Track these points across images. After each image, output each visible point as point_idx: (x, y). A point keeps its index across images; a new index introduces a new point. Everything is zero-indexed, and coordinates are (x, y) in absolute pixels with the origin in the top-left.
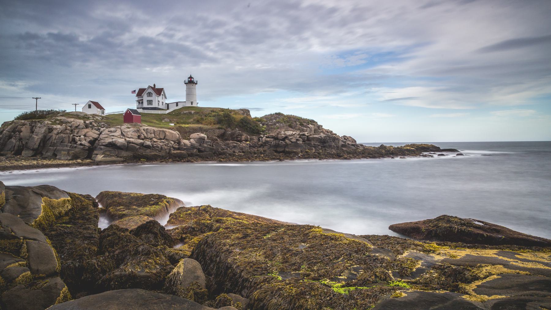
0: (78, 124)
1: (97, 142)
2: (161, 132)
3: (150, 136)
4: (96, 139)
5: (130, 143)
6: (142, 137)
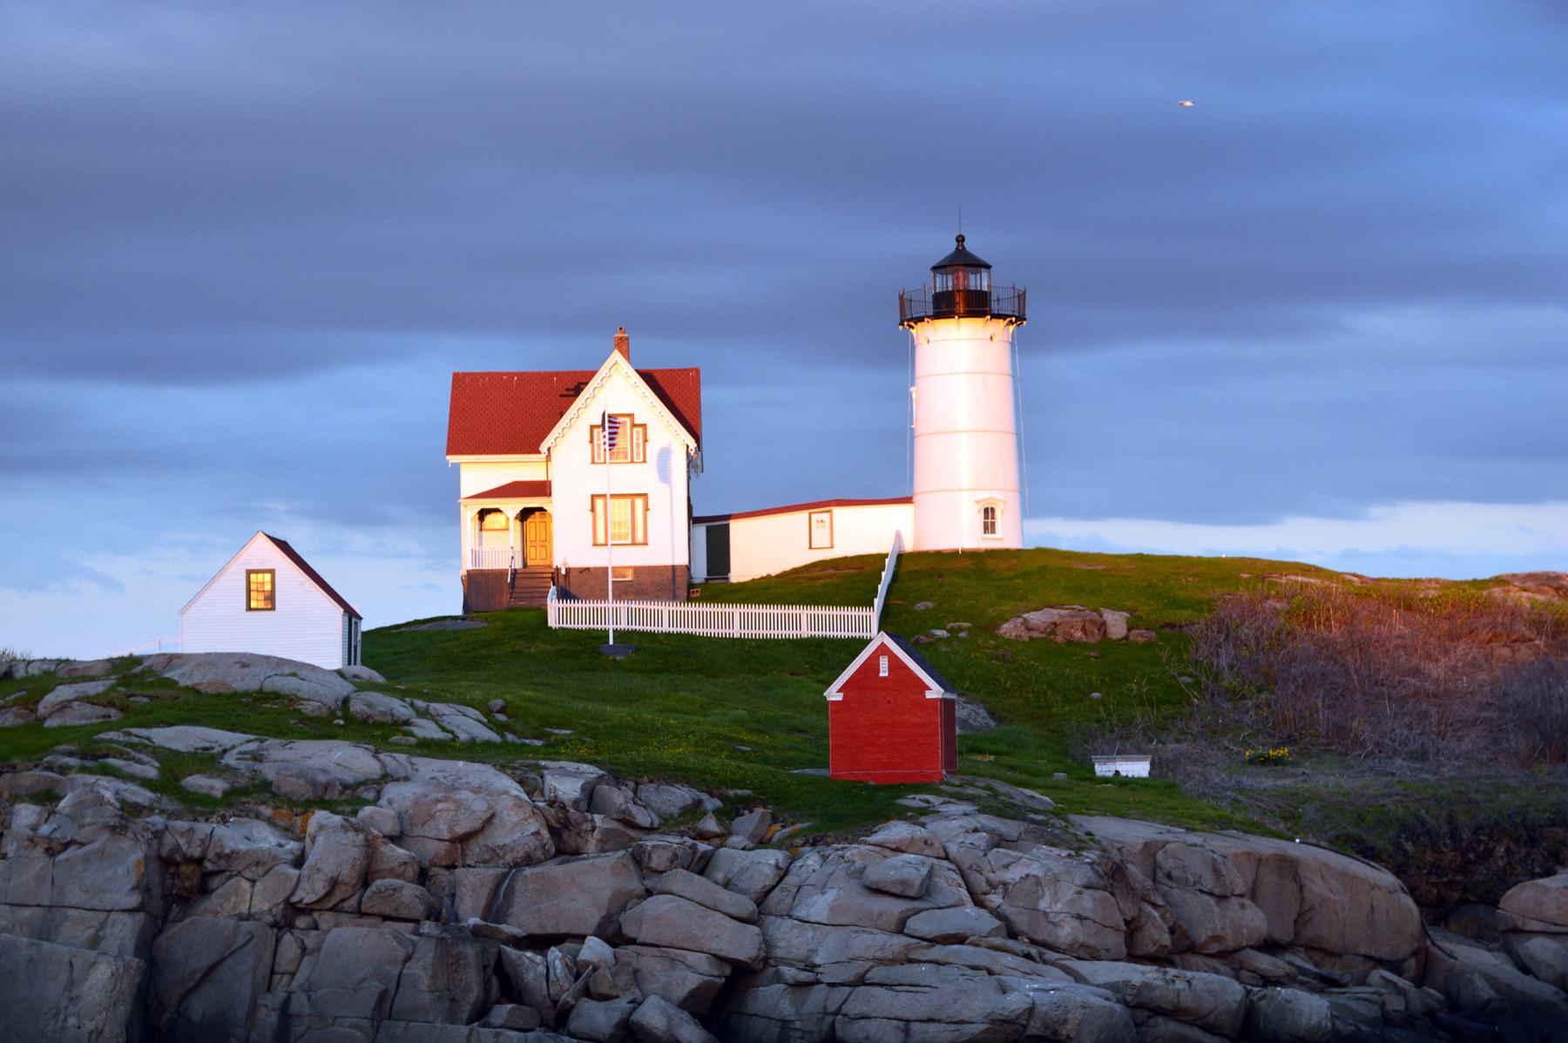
0: (479, 806)
1: (770, 999)
2: (1269, 878)
3: (1208, 920)
4: (740, 977)
5: (1158, 1011)
6: (1157, 934)
